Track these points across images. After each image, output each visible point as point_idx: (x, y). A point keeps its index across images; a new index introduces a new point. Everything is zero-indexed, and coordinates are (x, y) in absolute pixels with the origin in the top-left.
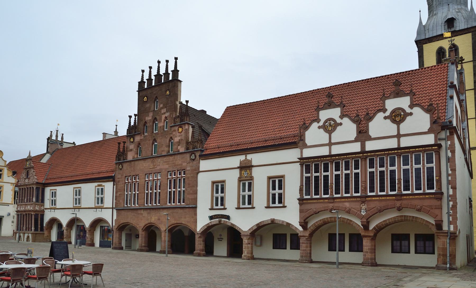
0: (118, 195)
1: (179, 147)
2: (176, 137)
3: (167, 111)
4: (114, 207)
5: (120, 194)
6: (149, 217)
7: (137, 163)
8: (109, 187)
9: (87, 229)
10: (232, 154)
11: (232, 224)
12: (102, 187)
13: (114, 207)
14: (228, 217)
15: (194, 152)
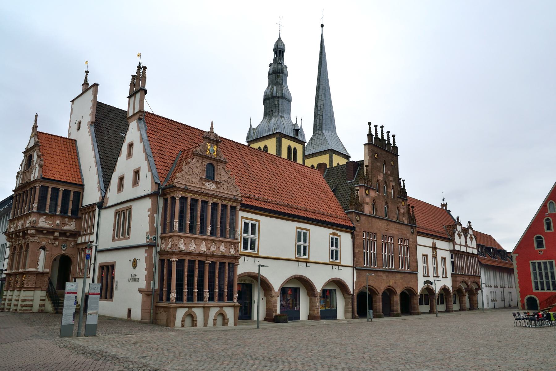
0: (357, 251)
5: (359, 251)
6: (388, 281)
7: (374, 220)
9: (318, 294)
10: (438, 238)
12: (337, 237)
15: (413, 228)
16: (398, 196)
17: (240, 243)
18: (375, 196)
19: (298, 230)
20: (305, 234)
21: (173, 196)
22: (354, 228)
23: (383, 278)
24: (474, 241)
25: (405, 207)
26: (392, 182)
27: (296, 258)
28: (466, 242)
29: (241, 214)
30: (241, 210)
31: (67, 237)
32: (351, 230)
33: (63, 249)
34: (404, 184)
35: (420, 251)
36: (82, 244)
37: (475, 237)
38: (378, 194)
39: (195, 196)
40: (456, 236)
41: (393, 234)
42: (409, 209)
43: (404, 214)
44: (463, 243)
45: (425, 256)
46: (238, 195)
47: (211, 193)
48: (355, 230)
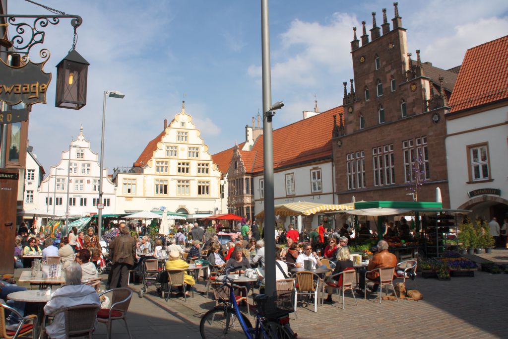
1: (414, 109)
2: (409, 97)
3: (392, 69)
4: (335, 191)
5: (341, 176)
8: (327, 169)
11: (504, 200)
12: (318, 170)
13: (335, 191)
14: (498, 192)
15: (437, 112)
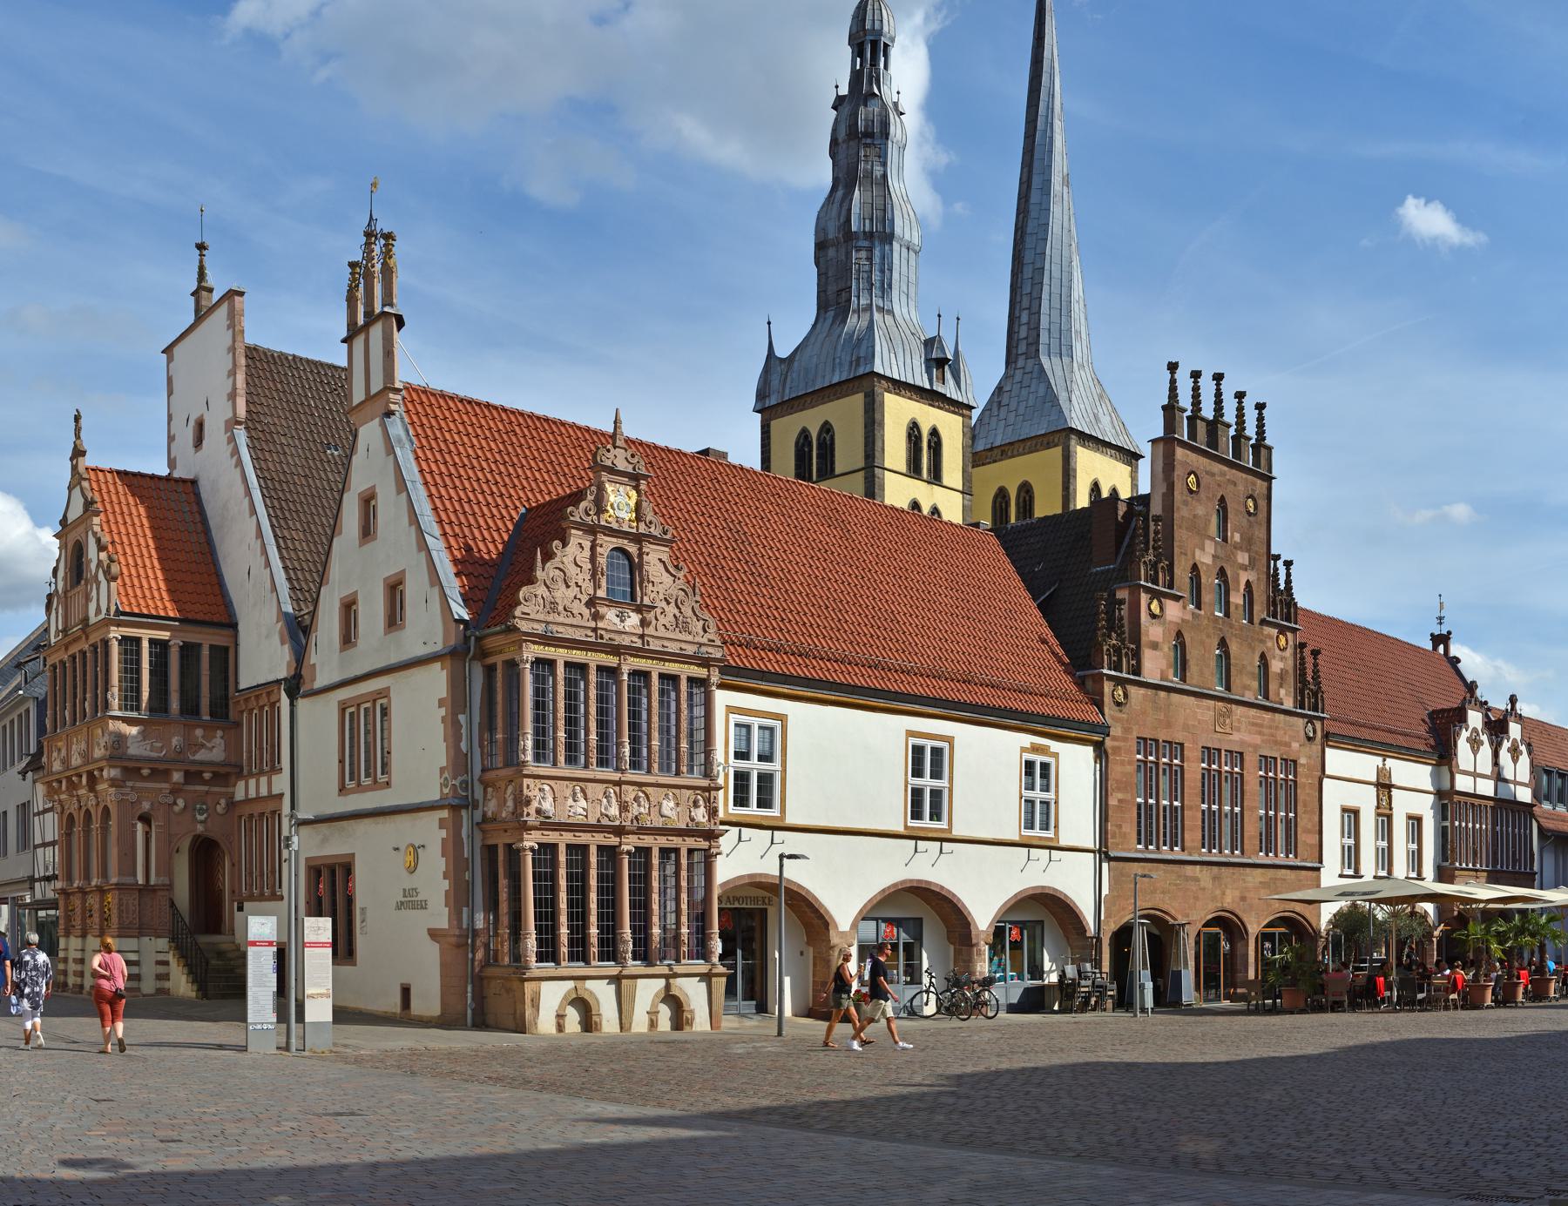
1: (1282, 692)
6: (1218, 892)
9: (982, 936)
16: (1264, 615)
17: (726, 788)
18: (1183, 620)
19: (912, 741)
20: (937, 752)
21: (511, 657)
22: (1104, 730)
23: (1203, 884)
24: (1524, 760)
25: (1289, 653)
26: (1245, 568)
27: (906, 827)
28: (1496, 763)
29: (722, 698)
30: (722, 686)
31: (205, 783)
32: (1095, 736)
33: (202, 818)
34: (1288, 575)
35: (1335, 797)
36: (248, 801)
37: (1529, 746)
38: (1193, 614)
39: (578, 656)
40: (1463, 746)
41: (1242, 742)
42: (1302, 658)
43: (1282, 676)
44: (1485, 766)
45: (1351, 814)
46: (710, 640)
47: (626, 641)
48: (1108, 735)
